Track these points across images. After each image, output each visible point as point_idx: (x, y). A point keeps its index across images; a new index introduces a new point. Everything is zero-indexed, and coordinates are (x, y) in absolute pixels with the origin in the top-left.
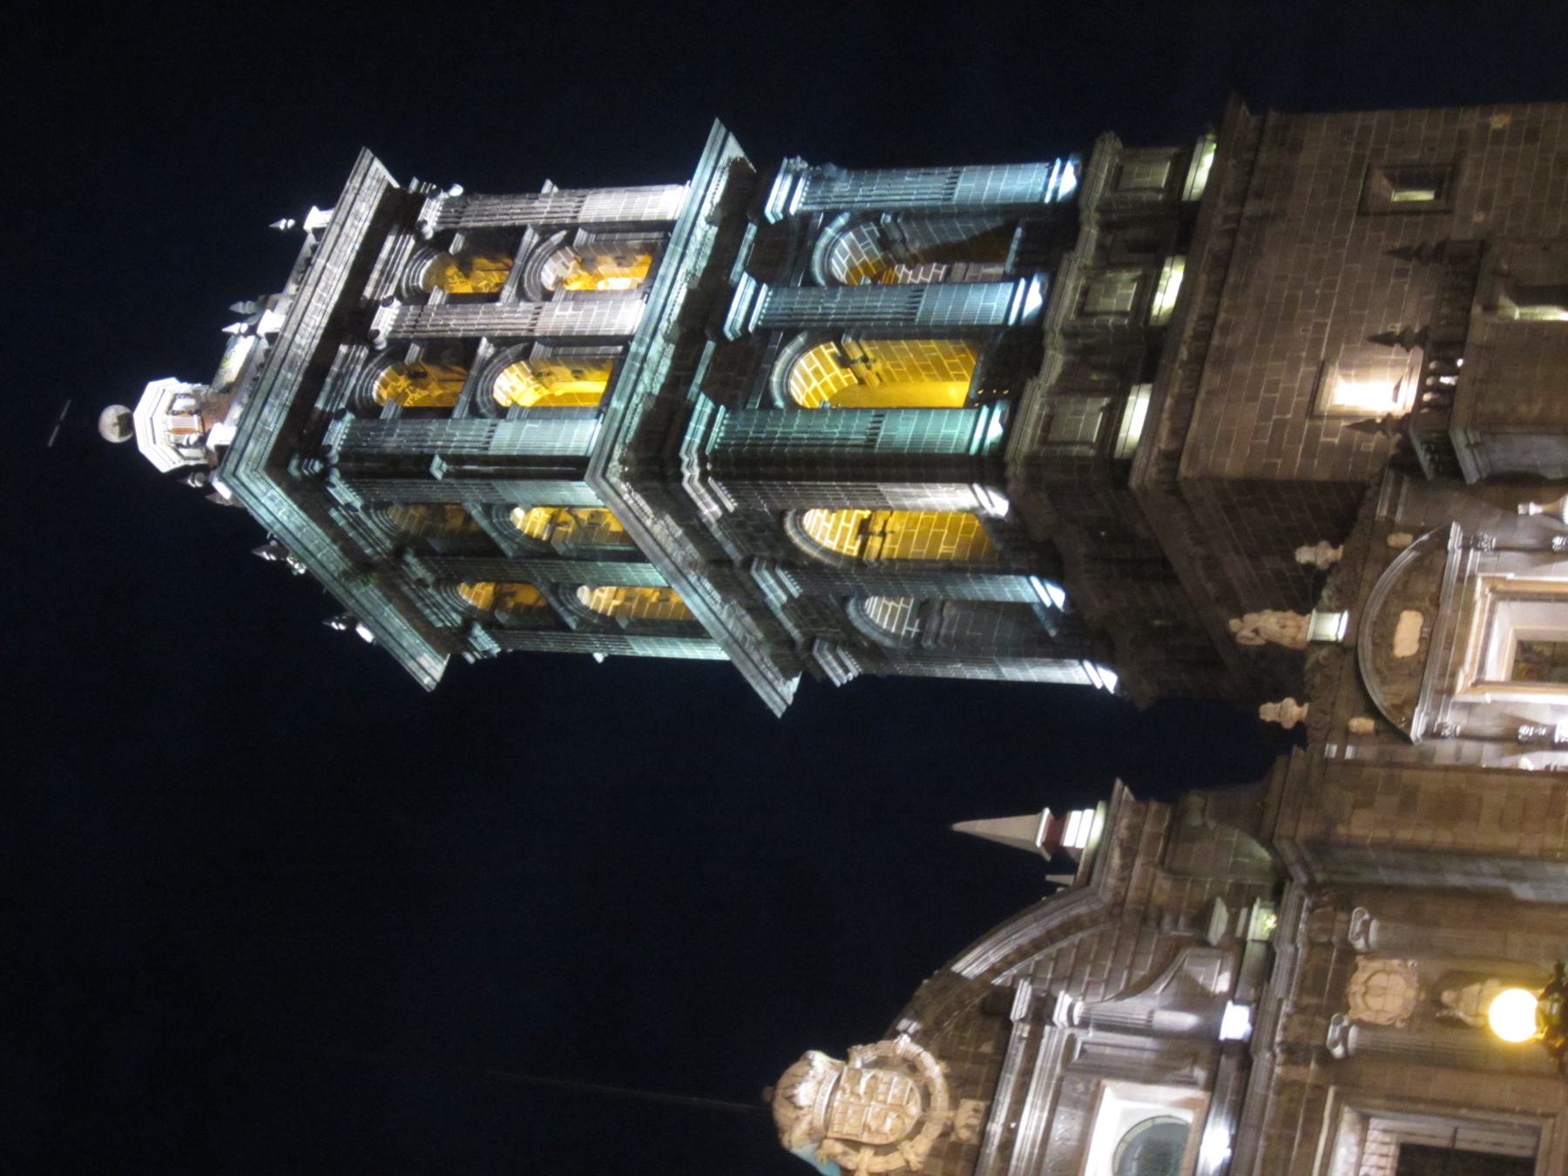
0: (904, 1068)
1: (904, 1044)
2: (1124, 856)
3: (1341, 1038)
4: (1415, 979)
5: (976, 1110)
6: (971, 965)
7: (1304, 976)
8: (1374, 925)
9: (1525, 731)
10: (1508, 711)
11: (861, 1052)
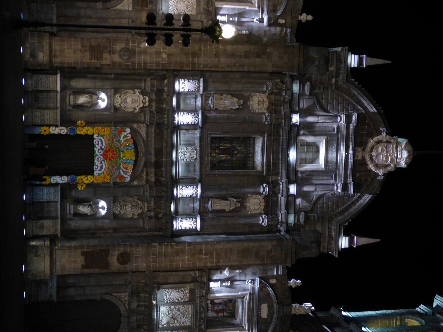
0: (379, 166)
1: (381, 173)
2: (331, 235)
3: (264, 189)
4: (248, 208)
5: (357, 156)
6: (367, 198)
7: (277, 206)
8: (261, 222)
9: (229, 284)
10: (234, 290)
11: (392, 169)
